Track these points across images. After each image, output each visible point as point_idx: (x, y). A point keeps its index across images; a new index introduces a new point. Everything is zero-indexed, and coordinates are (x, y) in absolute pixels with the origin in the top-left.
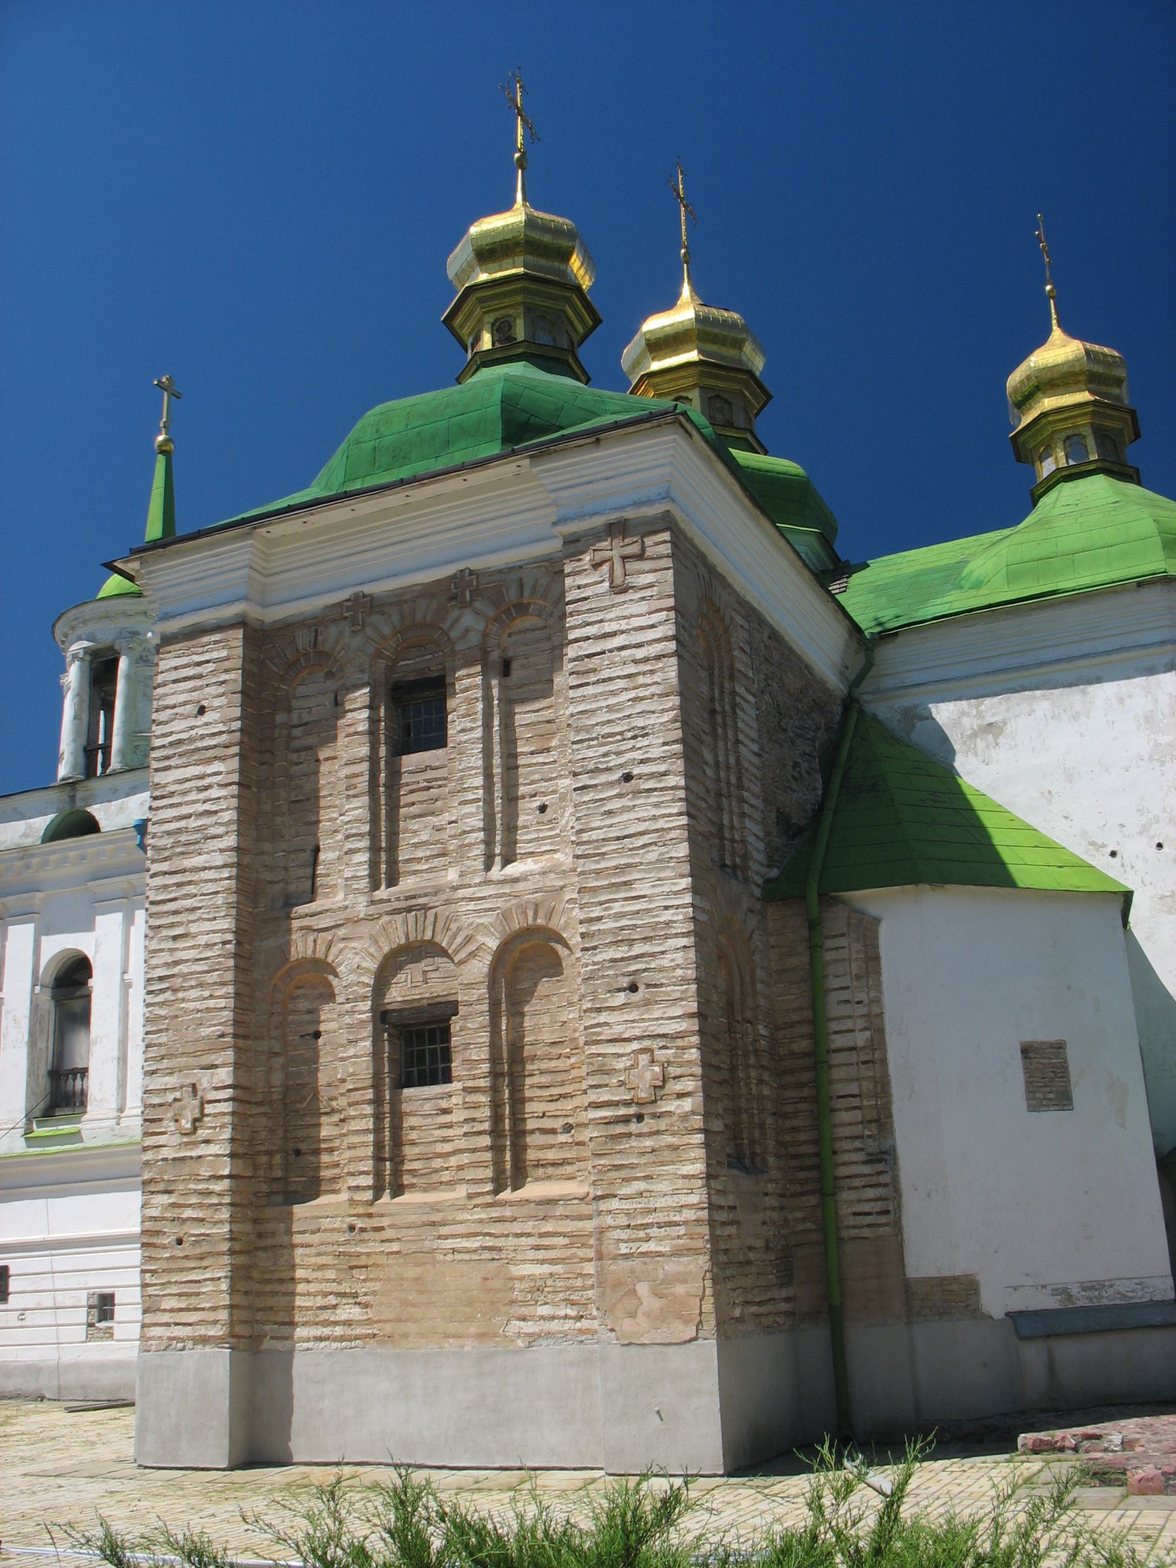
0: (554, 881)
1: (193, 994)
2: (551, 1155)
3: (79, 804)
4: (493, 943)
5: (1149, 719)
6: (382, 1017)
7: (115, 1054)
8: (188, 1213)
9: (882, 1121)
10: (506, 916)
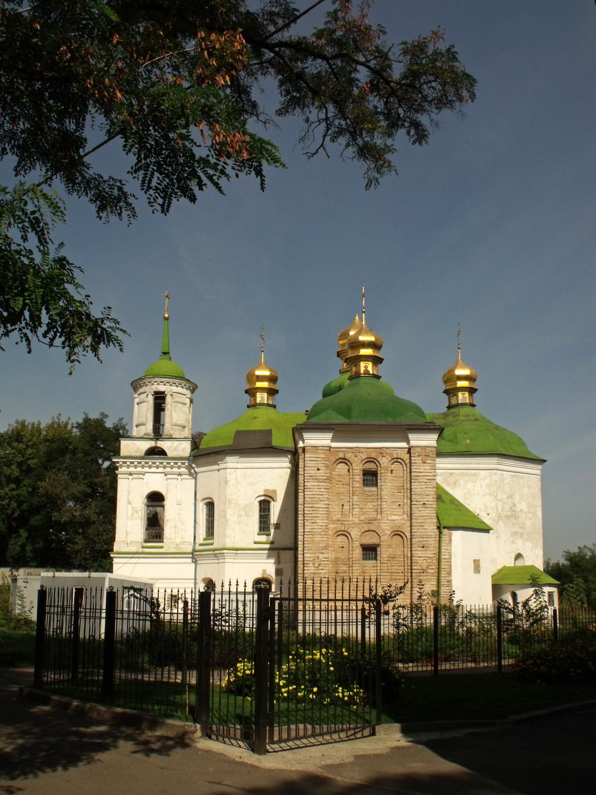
0: (403, 522)
2: (398, 577)
3: (158, 445)
4: (389, 533)
5: (489, 485)
6: (361, 545)
9: (450, 574)
10: (392, 527)
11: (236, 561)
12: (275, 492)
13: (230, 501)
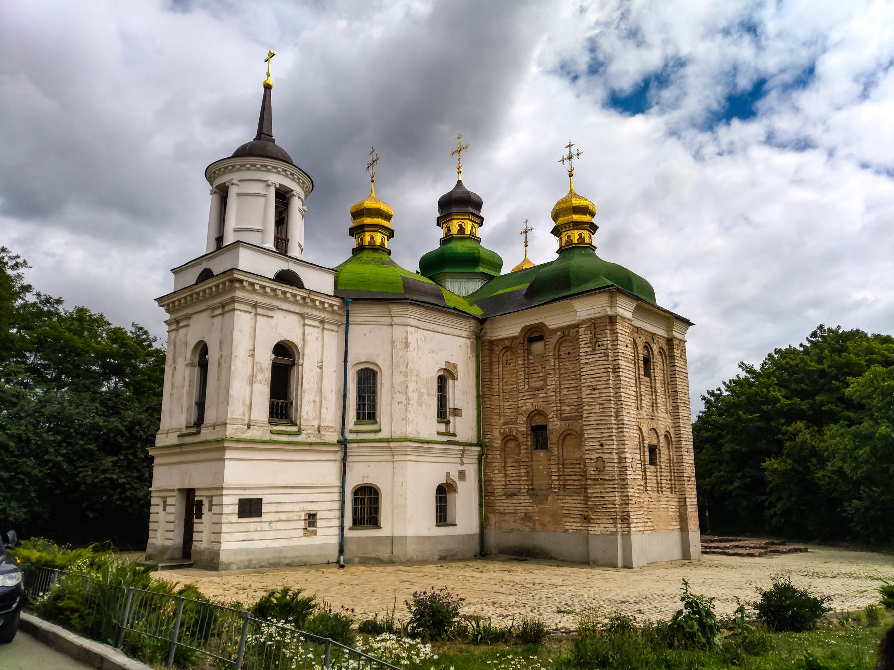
11: (420, 459)
12: (455, 366)
13: (411, 370)
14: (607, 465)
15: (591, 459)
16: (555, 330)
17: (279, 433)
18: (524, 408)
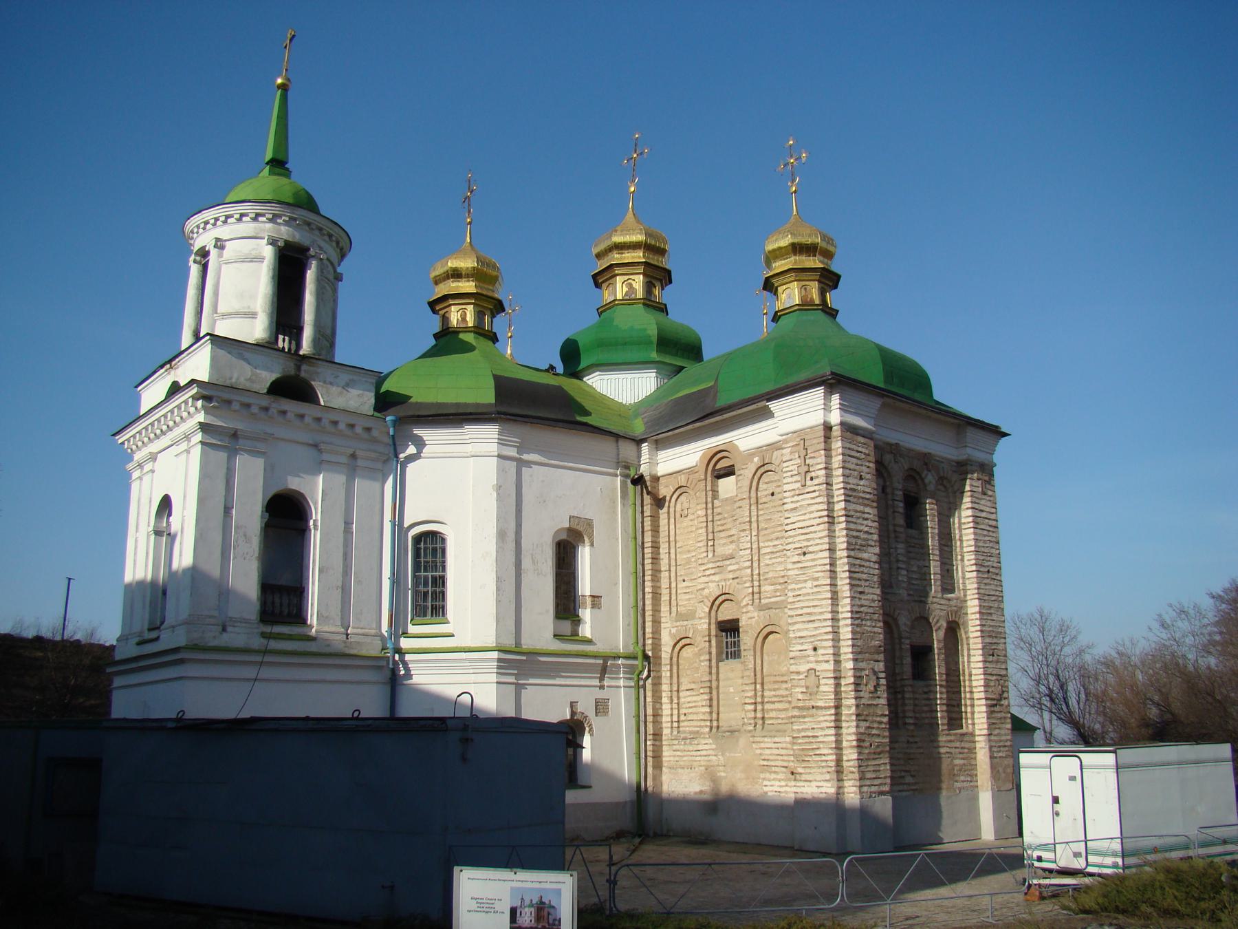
1: (869, 623)
3: (303, 374)
6: (913, 647)
7: (340, 584)
8: (874, 732)
14: (822, 682)
15: (798, 673)
16: (751, 454)
17: (280, 637)
18: (706, 591)
